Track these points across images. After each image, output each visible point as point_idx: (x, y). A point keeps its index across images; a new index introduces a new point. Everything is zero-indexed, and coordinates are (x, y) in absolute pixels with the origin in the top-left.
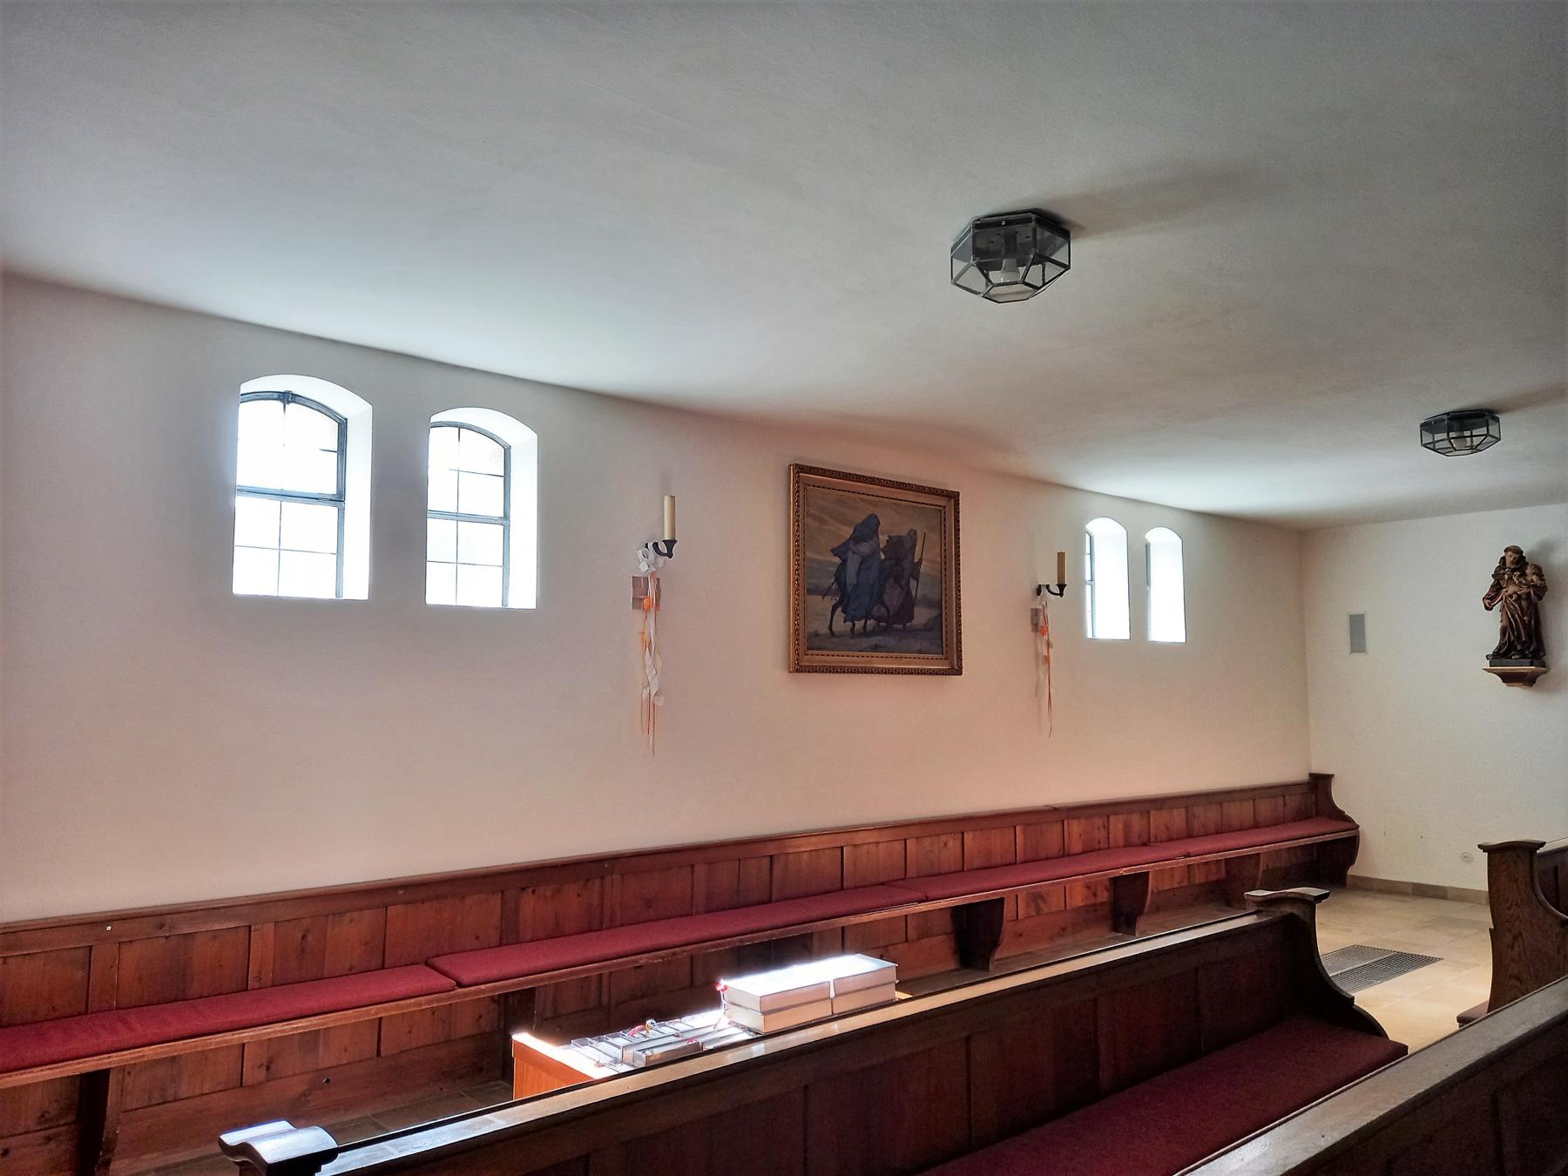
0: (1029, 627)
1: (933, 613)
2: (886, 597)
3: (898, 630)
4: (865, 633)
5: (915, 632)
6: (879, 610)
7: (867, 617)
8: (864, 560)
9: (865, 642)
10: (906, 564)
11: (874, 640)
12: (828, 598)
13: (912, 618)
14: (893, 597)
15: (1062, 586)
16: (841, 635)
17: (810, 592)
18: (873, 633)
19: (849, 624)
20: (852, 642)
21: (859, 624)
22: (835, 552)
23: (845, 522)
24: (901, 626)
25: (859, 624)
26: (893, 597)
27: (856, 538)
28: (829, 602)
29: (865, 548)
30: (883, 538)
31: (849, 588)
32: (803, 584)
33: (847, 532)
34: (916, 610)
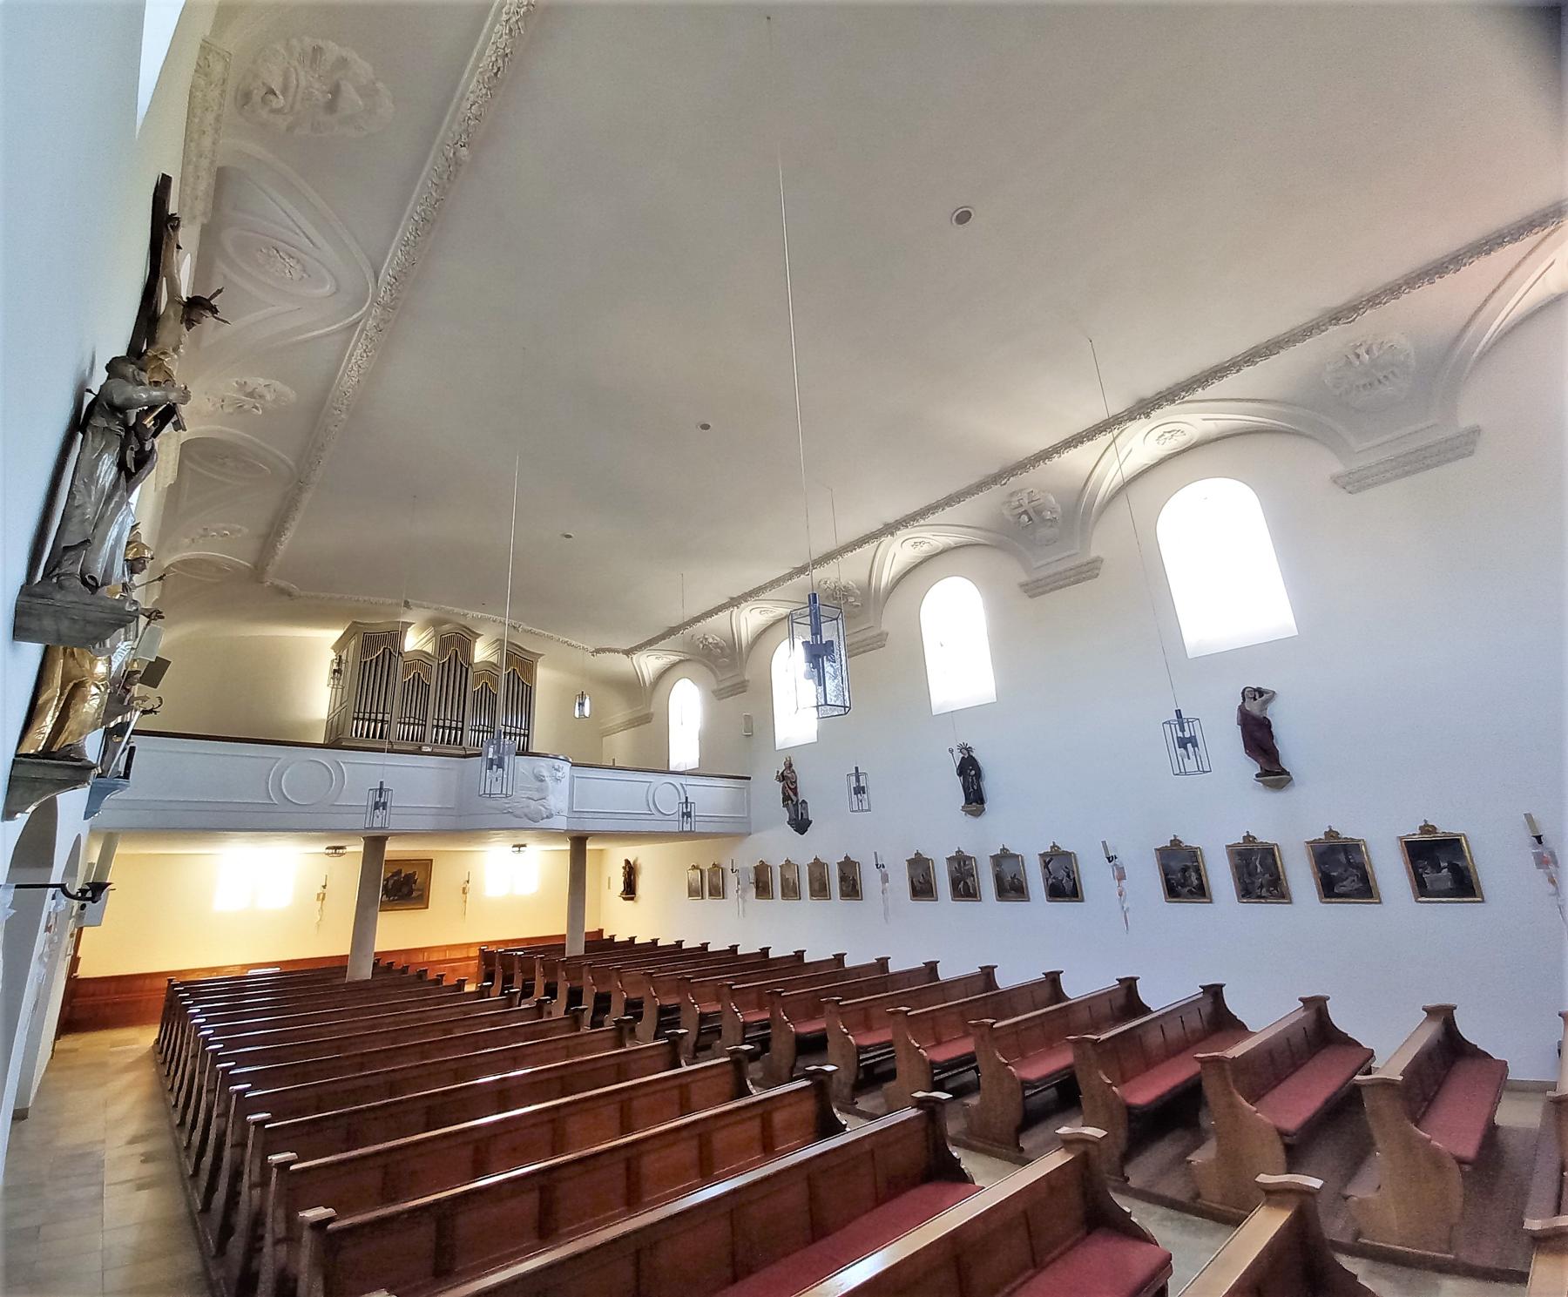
2: (403, 890)
4: (393, 900)
6: (400, 894)
7: (395, 896)
14: (405, 890)
30: (403, 875)
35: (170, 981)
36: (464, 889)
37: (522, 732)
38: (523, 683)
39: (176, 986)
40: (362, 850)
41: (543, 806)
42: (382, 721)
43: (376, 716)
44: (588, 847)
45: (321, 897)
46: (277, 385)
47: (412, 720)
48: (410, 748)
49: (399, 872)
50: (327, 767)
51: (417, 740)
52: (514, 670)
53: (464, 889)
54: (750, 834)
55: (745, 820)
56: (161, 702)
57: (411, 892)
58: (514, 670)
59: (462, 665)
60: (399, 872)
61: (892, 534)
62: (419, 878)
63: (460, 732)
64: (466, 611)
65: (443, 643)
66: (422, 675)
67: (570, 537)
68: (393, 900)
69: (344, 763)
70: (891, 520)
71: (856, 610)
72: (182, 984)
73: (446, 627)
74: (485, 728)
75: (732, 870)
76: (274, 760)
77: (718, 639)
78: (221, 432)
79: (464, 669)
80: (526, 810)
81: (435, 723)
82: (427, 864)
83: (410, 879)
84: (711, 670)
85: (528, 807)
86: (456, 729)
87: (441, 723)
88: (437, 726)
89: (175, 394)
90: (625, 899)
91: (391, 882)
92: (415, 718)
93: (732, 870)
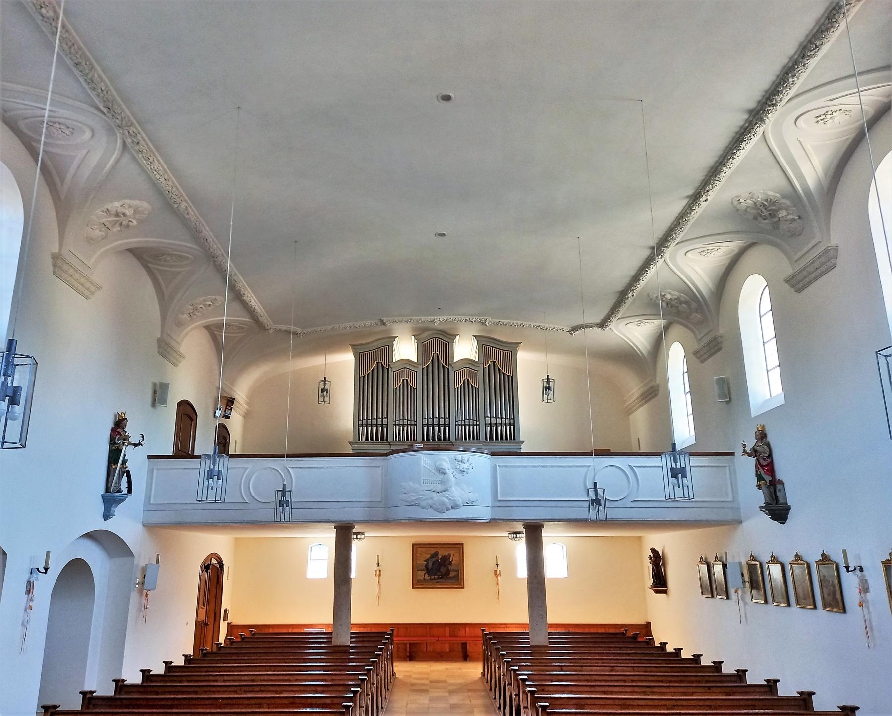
1: (456, 573)
2: (441, 570)
4: (434, 579)
9: (434, 581)
10: (447, 562)
11: (437, 581)
13: (449, 574)
14: (443, 570)
15: (46, 569)
16: (427, 580)
17: (418, 570)
18: (438, 578)
19: (430, 577)
21: (433, 577)
22: (425, 561)
23: (428, 554)
25: (433, 577)
28: (423, 573)
29: (434, 560)
30: (440, 557)
31: (429, 569)
32: (416, 569)
33: (429, 556)
34: (451, 573)
38: (504, 374)
40: (335, 535)
41: (447, 497)
42: (382, 425)
43: (363, 422)
44: (543, 534)
45: (377, 573)
46: (127, 201)
47: (413, 422)
48: (406, 447)
49: (436, 554)
50: (281, 474)
51: (411, 439)
52: (494, 362)
54: (740, 522)
55: (730, 505)
56: (143, 438)
57: (448, 572)
58: (494, 362)
60: (436, 554)
61: (762, 121)
62: (454, 560)
63: (447, 428)
64: (432, 318)
65: (423, 350)
66: (409, 381)
67: (443, 235)
68: (434, 579)
70: (752, 104)
71: (793, 225)
73: (426, 334)
74: (471, 422)
75: (847, 568)
76: (244, 470)
77: (676, 293)
78: (139, 242)
80: (430, 502)
82: (459, 547)
83: (446, 560)
84: (686, 326)
85: (432, 499)
86: (444, 425)
87: (431, 421)
88: (427, 425)
89: (137, 217)
90: (657, 592)
92: (414, 421)
93: (847, 568)
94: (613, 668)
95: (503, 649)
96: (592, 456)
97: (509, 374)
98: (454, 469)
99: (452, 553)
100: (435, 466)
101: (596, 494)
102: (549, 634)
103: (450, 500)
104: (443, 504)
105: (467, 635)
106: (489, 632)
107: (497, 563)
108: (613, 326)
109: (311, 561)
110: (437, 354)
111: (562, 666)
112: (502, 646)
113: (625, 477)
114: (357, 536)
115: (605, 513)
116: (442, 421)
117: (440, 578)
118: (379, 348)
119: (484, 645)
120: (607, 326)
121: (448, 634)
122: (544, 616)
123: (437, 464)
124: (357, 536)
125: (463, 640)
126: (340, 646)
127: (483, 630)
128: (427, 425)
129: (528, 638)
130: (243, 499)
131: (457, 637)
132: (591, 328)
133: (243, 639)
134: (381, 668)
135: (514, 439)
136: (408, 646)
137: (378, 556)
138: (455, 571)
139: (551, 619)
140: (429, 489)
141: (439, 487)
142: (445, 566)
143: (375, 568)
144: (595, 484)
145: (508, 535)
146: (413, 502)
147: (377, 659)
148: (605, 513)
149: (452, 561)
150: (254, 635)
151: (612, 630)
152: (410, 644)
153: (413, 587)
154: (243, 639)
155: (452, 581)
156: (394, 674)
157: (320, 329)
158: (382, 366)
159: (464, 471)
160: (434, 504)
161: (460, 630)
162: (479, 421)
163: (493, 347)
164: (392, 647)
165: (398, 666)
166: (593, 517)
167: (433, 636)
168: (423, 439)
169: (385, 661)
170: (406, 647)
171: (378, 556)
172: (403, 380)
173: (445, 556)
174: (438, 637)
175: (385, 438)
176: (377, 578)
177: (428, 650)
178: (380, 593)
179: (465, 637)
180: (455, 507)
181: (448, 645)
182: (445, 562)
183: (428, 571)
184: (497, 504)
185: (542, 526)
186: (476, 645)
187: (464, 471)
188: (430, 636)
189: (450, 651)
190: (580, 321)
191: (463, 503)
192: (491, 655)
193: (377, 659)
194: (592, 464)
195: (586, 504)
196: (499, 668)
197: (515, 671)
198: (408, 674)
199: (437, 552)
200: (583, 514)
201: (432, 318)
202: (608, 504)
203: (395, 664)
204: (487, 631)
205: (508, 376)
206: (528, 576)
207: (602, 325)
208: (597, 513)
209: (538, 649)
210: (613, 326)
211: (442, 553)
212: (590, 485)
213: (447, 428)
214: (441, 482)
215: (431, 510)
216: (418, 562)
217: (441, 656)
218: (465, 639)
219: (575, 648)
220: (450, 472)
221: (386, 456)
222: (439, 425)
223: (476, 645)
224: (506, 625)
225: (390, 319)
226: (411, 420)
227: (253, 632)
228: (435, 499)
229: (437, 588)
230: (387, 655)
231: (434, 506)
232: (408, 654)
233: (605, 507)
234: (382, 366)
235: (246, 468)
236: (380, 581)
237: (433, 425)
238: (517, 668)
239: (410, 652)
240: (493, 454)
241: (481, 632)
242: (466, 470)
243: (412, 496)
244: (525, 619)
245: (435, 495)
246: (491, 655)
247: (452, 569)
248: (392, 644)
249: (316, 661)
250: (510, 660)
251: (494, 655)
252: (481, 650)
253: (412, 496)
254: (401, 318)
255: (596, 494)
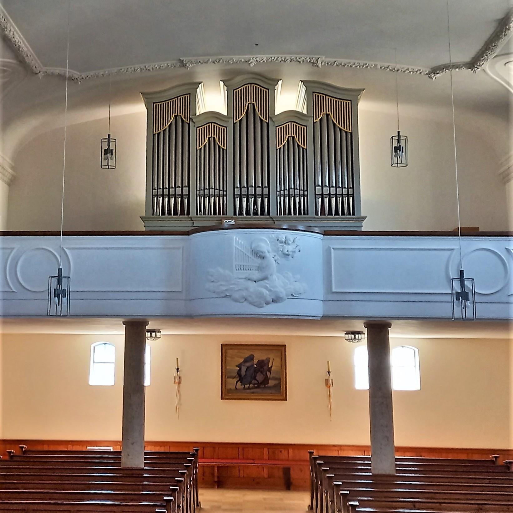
0: (325, 385)
2: (257, 378)
3: (261, 387)
4: (249, 388)
5: (270, 388)
7: (250, 383)
8: (248, 368)
9: (248, 391)
10: (265, 368)
11: (252, 390)
12: (234, 379)
13: (268, 383)
14: (260, 377)
16: (239, 389)
18: (252, 388)
19: (243, 386)
20: (244, 391)
21: (247, 386)
22: (237, 366)
23: (241, 358)
24: (263, 386)
25: (247, 386)
26: (260, 377)
27: (246, 361)
28: (235, 380)
29: (248, 364)
30: (256, 361)
31: (243, 376)
32: (225, 375)
33: (241, 360)
34: (270, 381)
35: (311, 453)
36: (327, 381)
37: (345, 191)
38: (340, 130)
39: (316, 459)
40: (124, 333)
42: (182, 196)
44: (391, 335)
48: (212, 223)
49: (251, 358)
51: (219, 214)
52: (328, 115)
53: (327, 381)
58: (328, 115)
59: (261, 121)
60: (251, 358)
62: (275, 365)
63: (266, 200)
64: (247, 57)
66: (217, 140)
68: (249, 388)
69: (66, 248)
72: (320, 458)
73: (239, 79)
74: (297, 192)
76: (9, 251)
79: (265, 125)
80: (244, 293)
81: (237, 192)
82: (281, 349)
83: (263, 366)
87: (244, 191)
91: (244, 369)
94: (481, 506)
95: (337, 477)
96: (458, 236)
97: (348, 131)
98: (275, 251)
99: (271, 356)
100: (251, 248)
101: (462, 285)
102: (397, 460)
103: (270, 291)
104: (261, 296)
105: (291, 458)
106: (320, 456)
107: (329, 369)
108: (487, 67)
109: (94, 364)
110: (253, 104)
111: (415, 502)
112: (330, 467)
113: (499, 262)
114: (151, 334)
115: (474, 309)
116: (259, 191)
117: (256, 388)
118: (178, 97)
119: (312, 471)
120: (479, 66)
121: (266, 457)
122: (390, 437)
123: (253, 247)
124: (151, 334)
125: (287, 464)
126: (132, 469)
127: (311, 453)
128: (241, 196)
129: (369, 465)
130: (9, 287)
131: (278, 460)
132: (457, 69)
133: (12, 457)
134: (183, 497)
135: (354, 214)
136: (216, 469)
137: (177, 359)
138: (275, 379)
139: (399, 441)
140: (243, 276)
141: (256, 275)
142: (262, 372)
143: (174, 373)
144: (462, 272)
145: (344, 335)
146: (222, 292)
147: (178, 488)
148: (474, 309)
149: (272, 366)
150: (25, 452)
151: (477, 455)
152: (219, 467)
153: (222, 398)
154: (12, 457)
155: (270, 391)
156: (198, 504)
157: (102, 73)
158: (182, 121)
159: (289, 255)
160: (250, 296)
161: (281, 452)
162: (307, 190)
163: (326, 95)
164: (196, 472)
165: (202, 494)
166: (458, 315)
167: (248, 459)
168: (235, 214)
169: (187, 488)
170: (214, 470)
171: (177, 359)
172: (209, 138)
173: (263, 361)
174: (254, 460)
175: (186, 212)
176: (177, 386)
177: (241, 475)
178: (181, 404)
179: (288, 460)
180: (276, 300)
181: (266, 471)
182: (262, 367)
183: (241, 378)
184: (331, 297)
185: (389, 325)
186: (301, 471)
187: (289, 255)
188: (244, 459)
189: (269, 477)
190: (444, 60)
191: (287, 295)
192: (321, 485)
193: (178, 488)
194: (458, 247)
195: (449, 298)
196: (332, 501)
197: (354, 507)
198: (216, 504)
199: (253, 355)
200: (445, 311)
201: (247, 57)
202: (478, 299)
203: (200, 491)
204: (315, 455)
205: (346, 132)
206: (370, 386)
207: (472, 64)
208: (464, 310)
209: (385, 479)
210: (487, 67)
211: (259, 356)
212: (454, 274)
213: (266, 200)
214: (259, 269)
215: (245, 303)
216: (228, 368)
217: (258, 483)
218: (287, 463)
219: (431, 480)
220: (270, 256)
221: (189, 235)
222: (255, 196)
223: (301, 471)
224: (340, 447)
225: (193, 59)
226: (219, 190)
227: (24, 449)
228: (251, 290)
229: (252, 399)
230: (190, 481)
231: (250, 299)
232: (216, 479)
233: (474, 302)
234: (182, 121)
235: (13, 249)
236: (181, 390)
237: (247, 196)
238: (357, 503)
239: (218, 477)
240: (326, 233)
241: (309, 454)
242: (291, 253)
243: (221, 285)
244: (366, 440)
245: (252, 286)
246: (321, 485)
247: (271, 376)
248: (196, 468)
249: (101, 487)
250: (348, 492)
251: (325, 483)
252: (308, 477)
253: (221, 285)
254: (206, 58)
255: (462, 285)
